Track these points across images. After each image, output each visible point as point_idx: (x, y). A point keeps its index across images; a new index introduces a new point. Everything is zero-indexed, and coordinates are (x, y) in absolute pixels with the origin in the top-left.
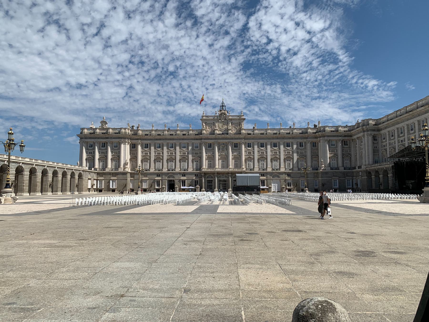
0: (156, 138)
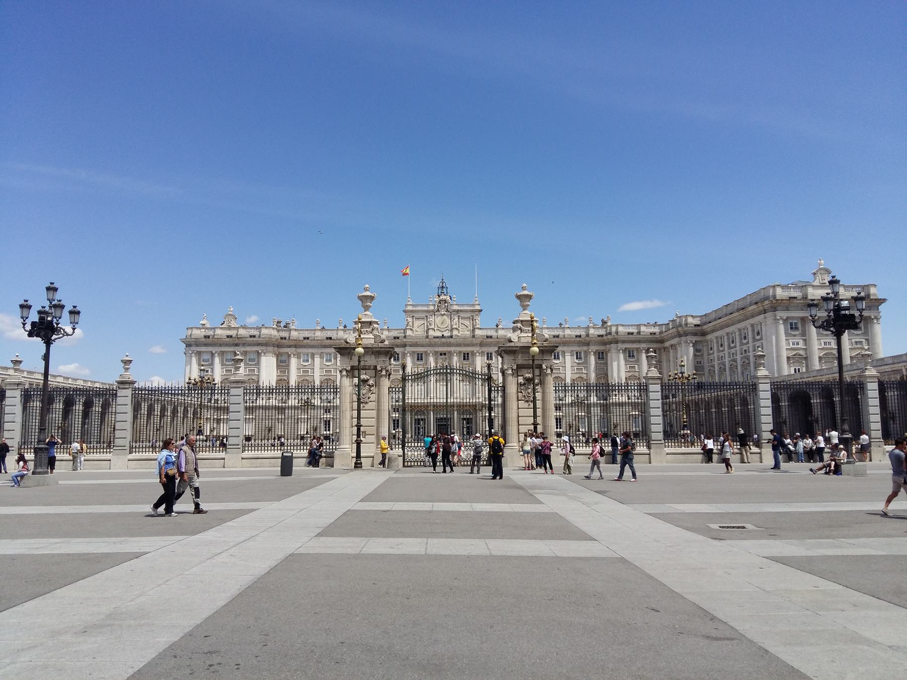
0: (324, 344)
